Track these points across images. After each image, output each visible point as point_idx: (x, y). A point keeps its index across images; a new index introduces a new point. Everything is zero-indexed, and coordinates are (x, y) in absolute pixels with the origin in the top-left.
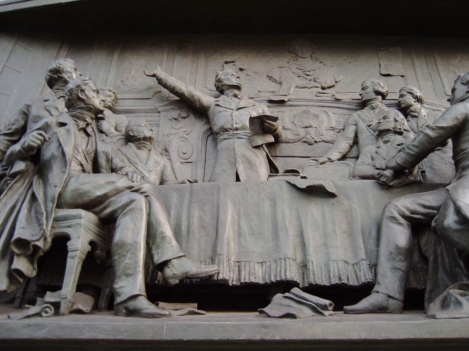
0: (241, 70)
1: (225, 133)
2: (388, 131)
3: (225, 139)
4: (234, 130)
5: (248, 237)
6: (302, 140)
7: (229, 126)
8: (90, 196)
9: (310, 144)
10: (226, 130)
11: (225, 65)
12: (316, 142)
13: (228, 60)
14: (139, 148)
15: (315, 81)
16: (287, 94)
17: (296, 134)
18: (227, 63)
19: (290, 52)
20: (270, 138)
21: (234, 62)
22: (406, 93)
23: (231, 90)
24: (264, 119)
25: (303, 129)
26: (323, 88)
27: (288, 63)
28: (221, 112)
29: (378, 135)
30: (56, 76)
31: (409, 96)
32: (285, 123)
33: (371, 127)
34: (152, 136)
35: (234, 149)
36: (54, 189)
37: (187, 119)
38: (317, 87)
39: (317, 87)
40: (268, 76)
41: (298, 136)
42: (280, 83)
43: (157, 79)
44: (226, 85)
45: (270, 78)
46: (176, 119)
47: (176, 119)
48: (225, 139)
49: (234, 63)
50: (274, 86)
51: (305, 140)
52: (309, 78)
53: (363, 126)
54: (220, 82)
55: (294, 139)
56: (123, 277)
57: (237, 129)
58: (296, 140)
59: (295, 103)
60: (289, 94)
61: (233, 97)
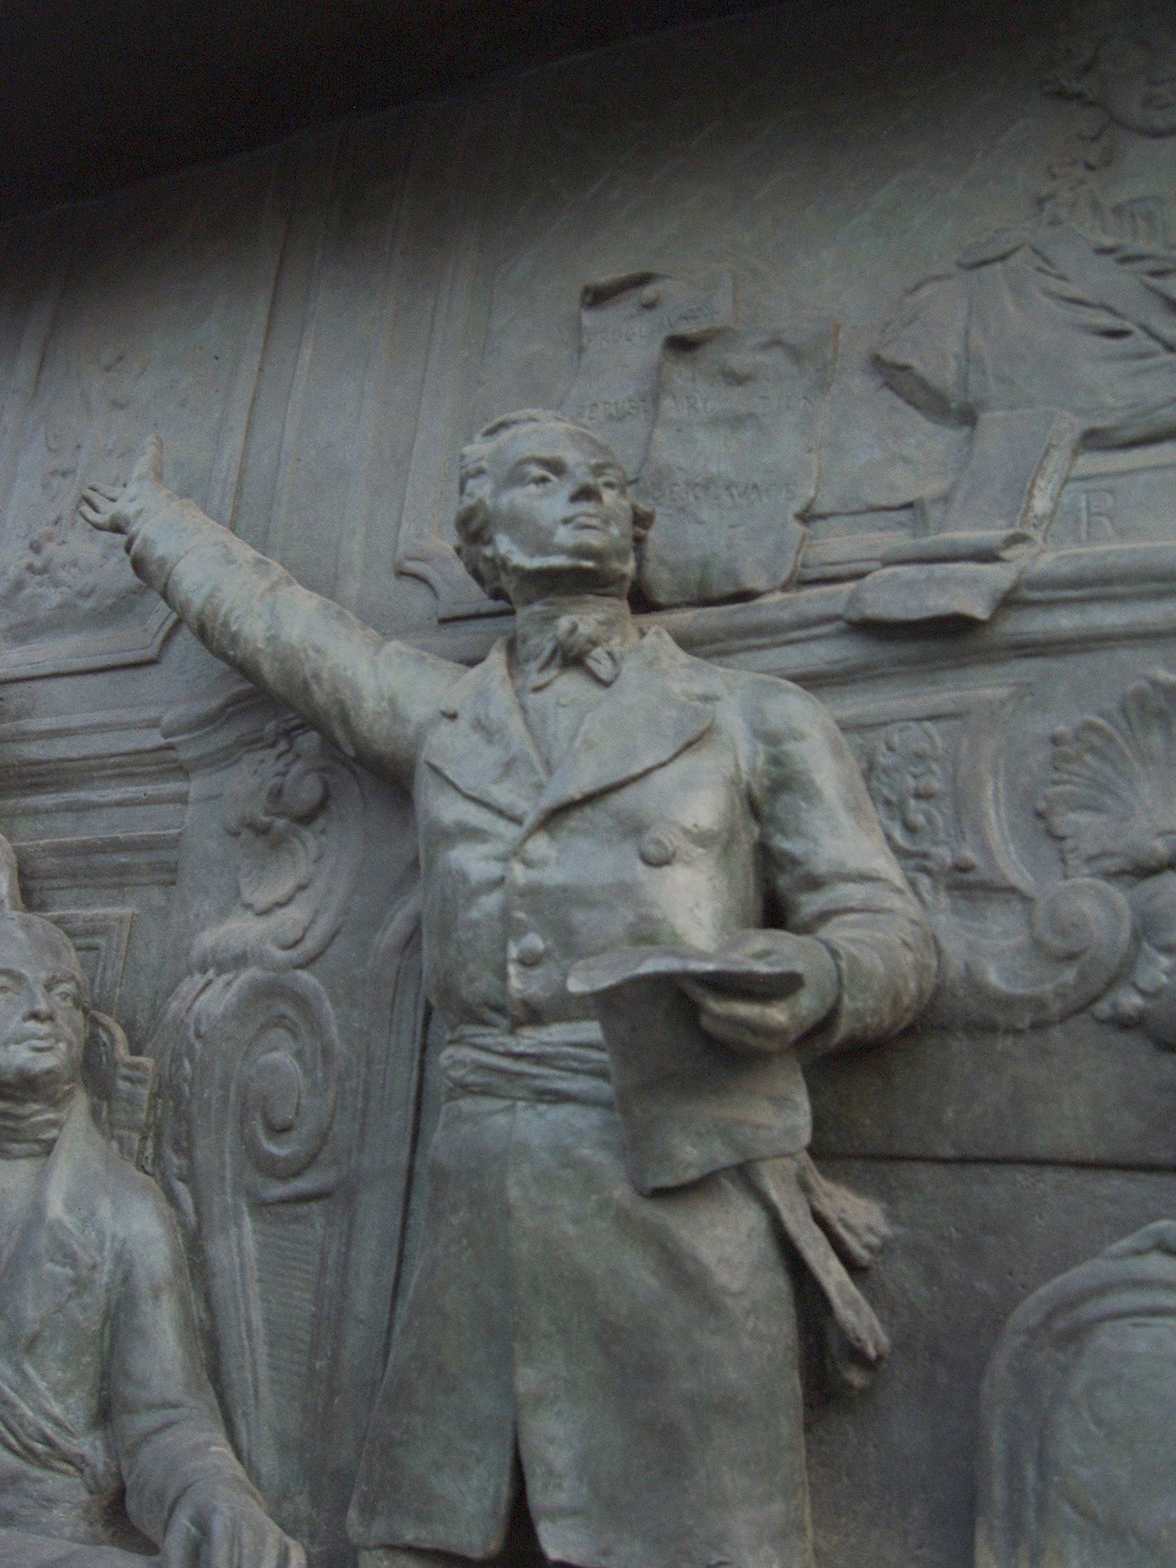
0: (681, 345)
1: (469, 1030)
4: (516, 1025)
6: (1103, 1008)
11: (589, 319)
13: (602, 276)
16: (991, 535)
17: (1057, 944)
18: (597, 297)
19: (1062, 95)
20: (780, 1102)
21: (643, 280)
25: (1118, 895)
27: (1040, 202)
32: (978, 830)
37: (320, 823)
40: (878, 364)
41: (1069, 975)
42: (968, 417)
45: (893, 375)
46: (262, 831)
47: (262, 831)
49: (648, 292)
50: (915, 456)
51: (1131, 1001)
55: (1038, 1004)
58: (1056, 1007)
59: (1066, 621)
60: (1017, 540)
61: (552, 672)
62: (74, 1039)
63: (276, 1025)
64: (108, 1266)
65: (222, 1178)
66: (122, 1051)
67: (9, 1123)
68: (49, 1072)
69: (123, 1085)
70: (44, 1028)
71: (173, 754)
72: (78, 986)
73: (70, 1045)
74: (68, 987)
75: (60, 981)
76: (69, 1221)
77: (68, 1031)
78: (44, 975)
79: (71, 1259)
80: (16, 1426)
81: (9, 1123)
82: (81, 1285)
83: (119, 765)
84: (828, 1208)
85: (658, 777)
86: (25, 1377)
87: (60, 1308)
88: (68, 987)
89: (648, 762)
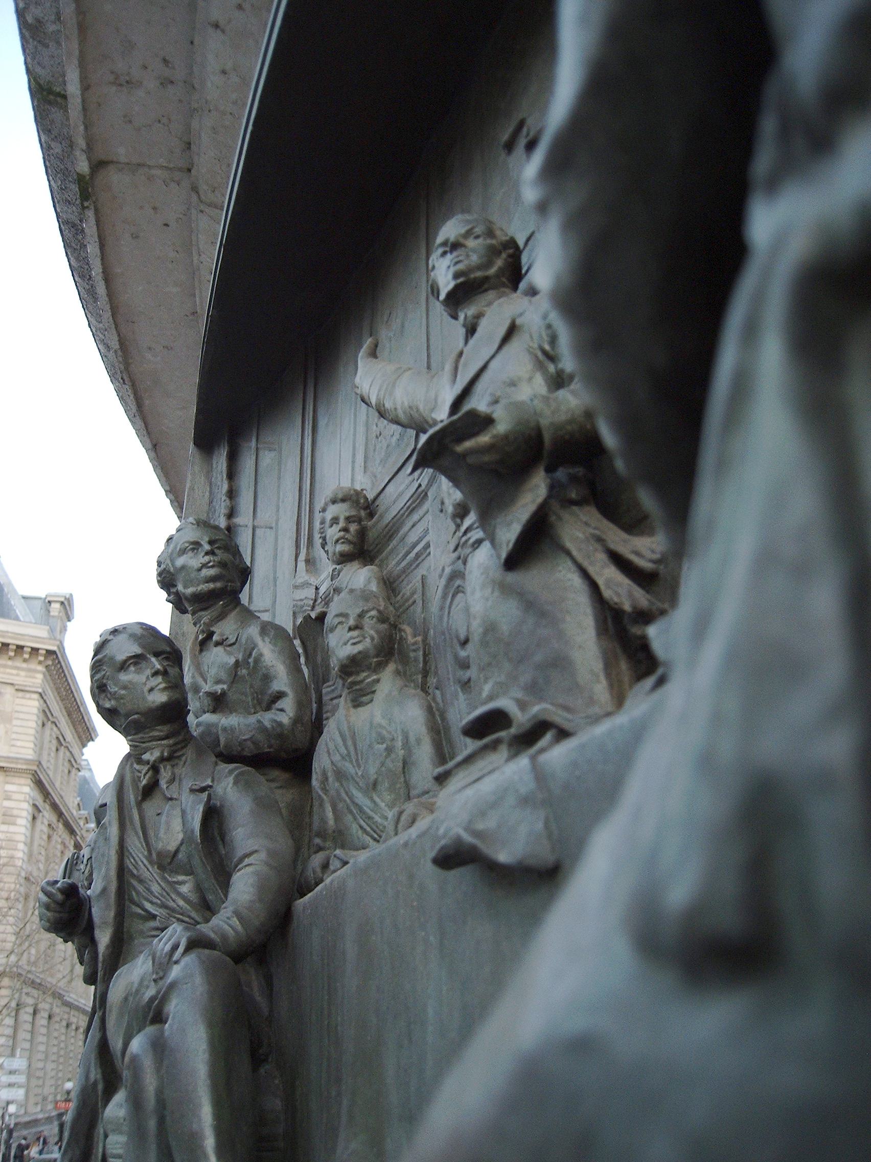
13: (505, 137)
14: (357, 704)
34: (360, 647)
62: (375, 636)
63: (457, 593)
64: (400, 738)
65: (449, 679)
66: (411, 640)
67: (358, 687)
68: (360, 652)
69: (412, 655)
70: (355, 633)
71: (420, 490)
72: (379, 611)
73: (372, 639)
74: (374, 613)
75: (367, 611)
76: (384, 723)
77: (372, 632)
78: (358, 611)
79: (382, 740)
80: (375, 828)
81: (358, 687)
82: (389, 750)
83: (409, 507)
84: (624, 550)
85: (493, 365)
86: (375, 802)
87: (383, 764)
88: (374, 613)
89: (487, 358)
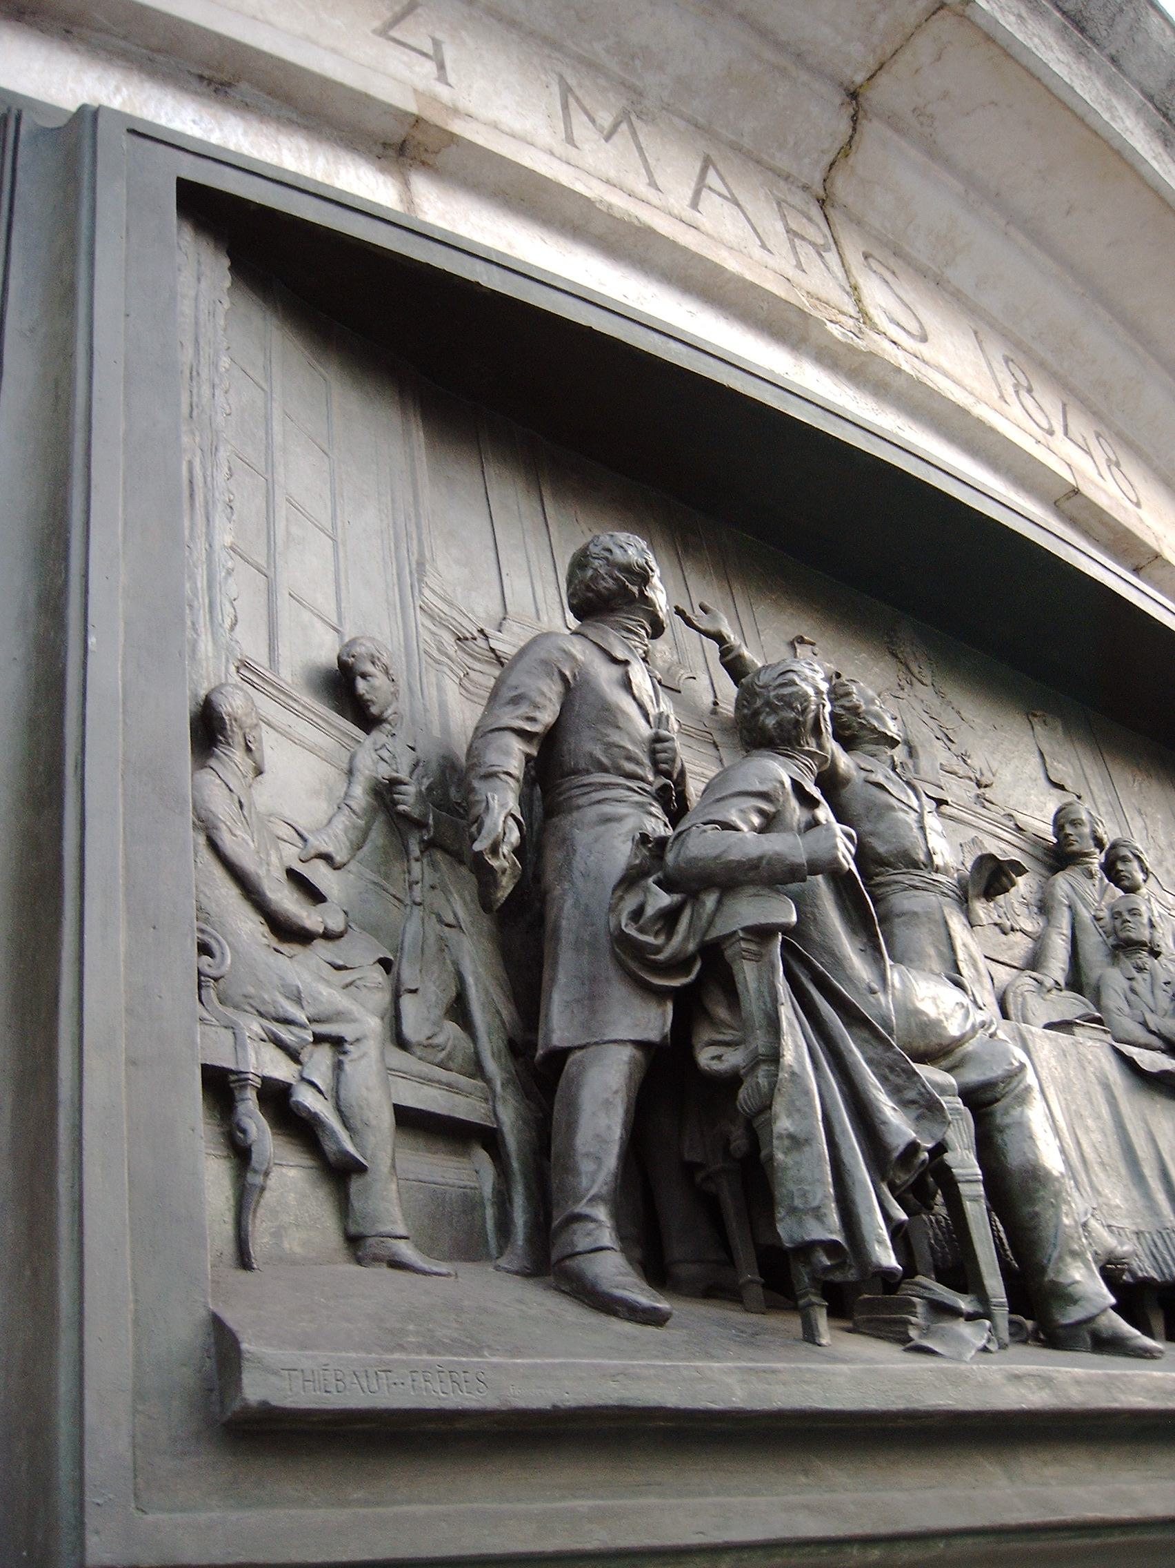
2: (1140, 944)
3: (916, 888)
5: (1097, 1168)
7: (922, 857)
8: (940, 1035)
9: (1005, 933)
10: (915, 864)
12: (1013, 929)
15: (964, 761)
18: (801, 640)
22: (1131, 856)
23: (882, 747)
24: (1006, 867)
26: (979, 785)
28: (892, 808)
29: (1115, 947)
30: (635, 589)
31: (1135, 864)
33: (1102, 923)
35: (946, 923)
36: (871, 998)
38: (970, 779)
39: (970, 779)
43: (723, 654)
44: (874, 730)
48: (916, 888)
52: (953, 747)
53: (1085, 915)
54: (858, 715)
56: (1069, 1259)
57: (937, 870)
